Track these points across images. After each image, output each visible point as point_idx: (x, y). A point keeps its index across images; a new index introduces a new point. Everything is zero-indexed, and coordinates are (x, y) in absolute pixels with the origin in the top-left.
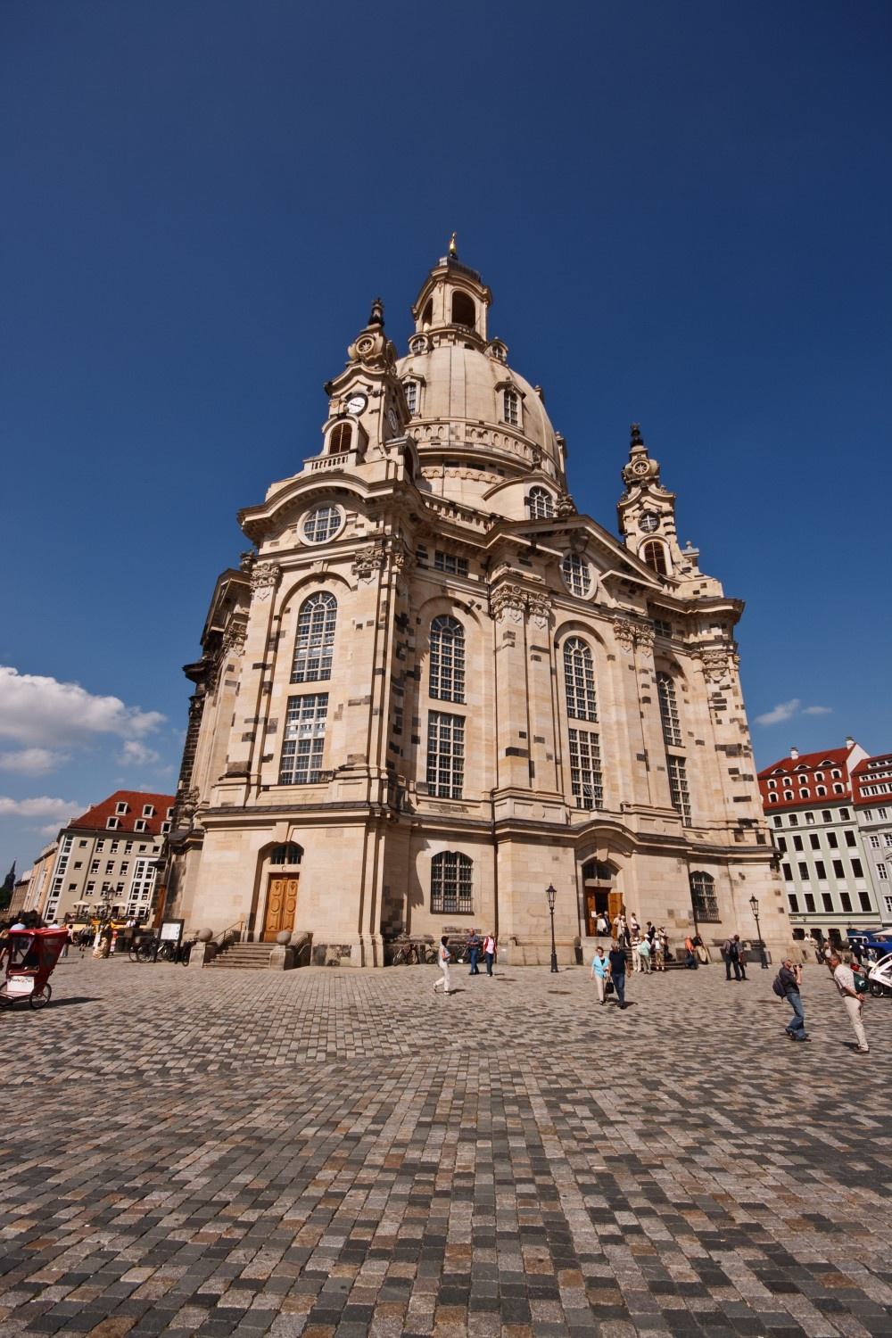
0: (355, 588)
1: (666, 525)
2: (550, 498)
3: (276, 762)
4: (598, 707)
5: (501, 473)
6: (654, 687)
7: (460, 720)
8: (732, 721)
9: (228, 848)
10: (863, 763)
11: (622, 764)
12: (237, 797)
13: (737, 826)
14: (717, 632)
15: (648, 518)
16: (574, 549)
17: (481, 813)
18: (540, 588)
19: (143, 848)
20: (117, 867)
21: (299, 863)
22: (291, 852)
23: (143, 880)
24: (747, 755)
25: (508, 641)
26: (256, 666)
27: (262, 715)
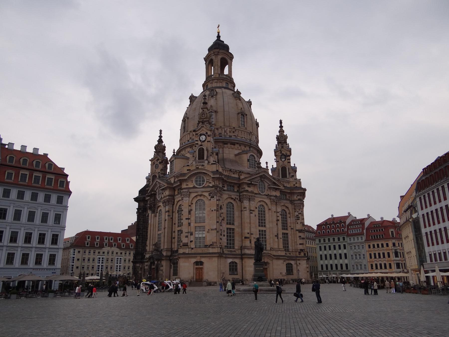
0: (210, 200)
1: (288, 159)
2: (255, 158)
3: (194, 242)
7: (233, 229)
8: (301, 223)
10: (353, 221)
14: (299, 197)
16: (261, 180)
17: (239, 252)
19: (99, 253)
20: (91, 259)
22: (202, 263)
23: (101, 264)
24: (303, 233)
26: (186, 219)
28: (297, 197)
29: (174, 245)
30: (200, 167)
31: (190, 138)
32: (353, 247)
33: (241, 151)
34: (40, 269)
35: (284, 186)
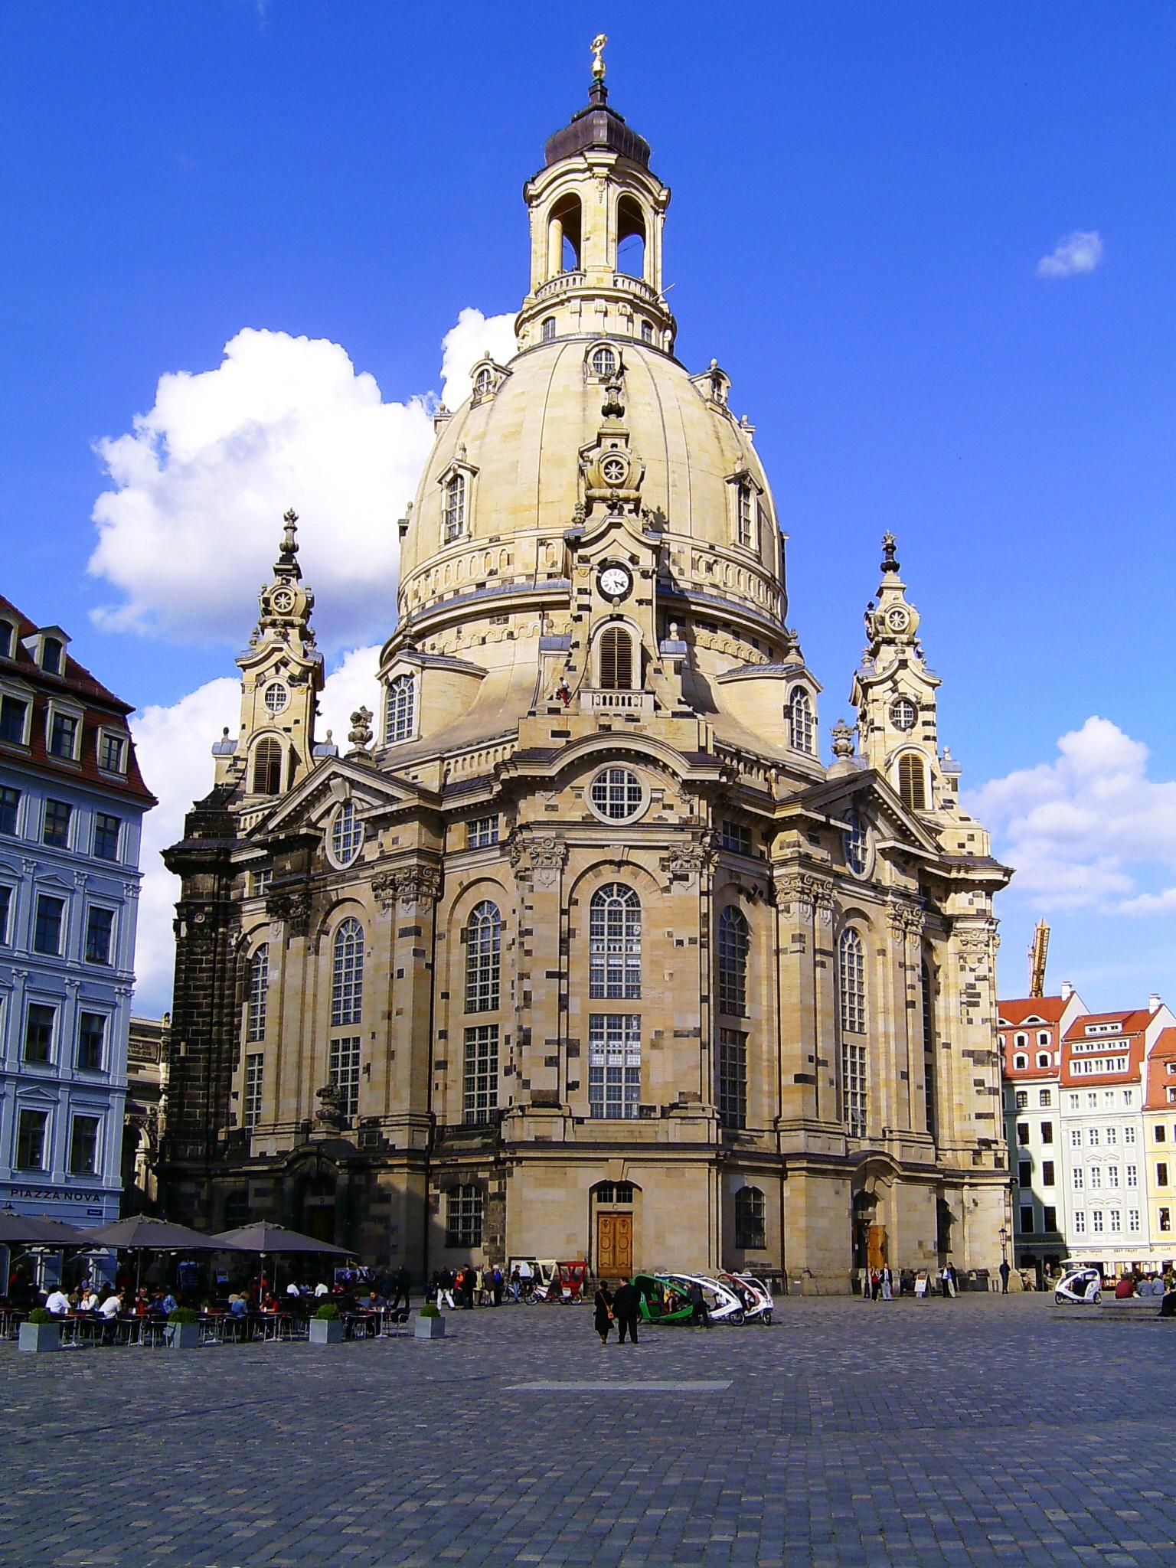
0: (667, 889)
1: (925, 723)
4: (866, 1014)
5: (737, 635)
6: (919, 985)
8: (984, 1021)
9: (548, 1186)
11: (887, 1080)
12: (555, 1131)
13: (976, 1147)
15: (902, 708)
16: (855, 809)
18: (829, 872)
21: (630, 1201)
24: (994, 1064)
25: (797, 946)
26: (550, 975)
27: (563, 1036)
28: (971, 902)
29: (445, 1100)
30: (618, 725)
31: (492, 573)
32: (1086, 1137)
33: (741, 663)
34: (39, 1189)
35: (939, 848)
